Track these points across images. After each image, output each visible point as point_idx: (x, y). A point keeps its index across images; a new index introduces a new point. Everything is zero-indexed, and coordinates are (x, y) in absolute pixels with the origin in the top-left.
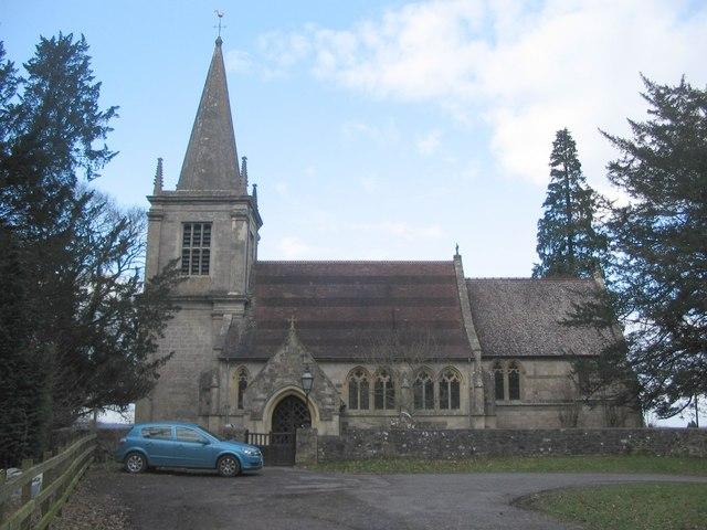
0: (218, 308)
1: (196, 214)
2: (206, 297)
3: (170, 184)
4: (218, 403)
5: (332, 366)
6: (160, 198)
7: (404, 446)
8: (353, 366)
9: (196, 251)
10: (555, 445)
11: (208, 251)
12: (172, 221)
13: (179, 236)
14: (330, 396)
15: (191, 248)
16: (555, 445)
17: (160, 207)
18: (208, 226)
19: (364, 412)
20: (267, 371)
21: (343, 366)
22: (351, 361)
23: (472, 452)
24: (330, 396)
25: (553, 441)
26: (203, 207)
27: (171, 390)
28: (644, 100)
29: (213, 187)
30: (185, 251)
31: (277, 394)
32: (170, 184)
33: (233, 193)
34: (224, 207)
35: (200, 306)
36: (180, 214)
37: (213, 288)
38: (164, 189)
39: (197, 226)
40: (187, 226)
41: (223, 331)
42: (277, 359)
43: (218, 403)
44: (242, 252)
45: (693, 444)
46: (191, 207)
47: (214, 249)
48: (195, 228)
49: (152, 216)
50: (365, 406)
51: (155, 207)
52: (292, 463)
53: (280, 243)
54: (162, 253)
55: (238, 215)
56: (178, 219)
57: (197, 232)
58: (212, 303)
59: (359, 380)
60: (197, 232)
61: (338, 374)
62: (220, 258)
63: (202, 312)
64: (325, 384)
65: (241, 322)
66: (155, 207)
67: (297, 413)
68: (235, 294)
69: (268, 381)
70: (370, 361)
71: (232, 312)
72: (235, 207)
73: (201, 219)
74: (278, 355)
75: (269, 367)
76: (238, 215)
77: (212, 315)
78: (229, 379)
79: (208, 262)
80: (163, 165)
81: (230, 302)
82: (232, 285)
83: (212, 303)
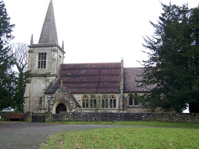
0: (48, 78)
1: (42, 50)
2: (44, 75)
3: (36, 42)
4: (44, 106)
5: (77, 95)
6: (32, 46)
7: (76, 117)
8: (83, 95)
9: (42, 61)
10: (121, 117)
11: (45, 61)
12: (35, 53)
13: (37, 57)
14: (72, 103)
15: (41, 61)
16: (121, 117)
17: (32, 49)
18: (46, 54)
19: (87, 108)
20: (54, 96)
21: (81, 95)
22: (83, 93)
23: (96, 119)
24: (72, 103)
25: (120, 116)
26: (44, 48)
27: (34, 102)
28: (31, 38)
29: (48, 42)
30: (39, 62)
31: (56, 103)
32: (36, 42)
33: (52, 43)
34: (50, 48)
35: (43, 78)
36: (38, 50)
37: (47, 72)
38: (33, 43)
39: (43, 54)
40: (40, 54)
41: (48, 85)
42: (57, 92)
43: (44, 106)
44: (55, 61)
45: (165, 117)
46: (41, 48)
47: (47, 61)
48: (45, 54)
49: (30, 52)
50: (87, 107)
51: (30, 49)
52: (44, 121)
53: (70, 59)
54: (32, 63)
55: (54, 50)
56: (37, 52)
57: (43, 56)
58: (46, 77)
59: (85, 99)
60: (43, 56)
61: (79, 97)
62: (49, 63)
63: (43, 79)
64: (71, 100)
65: (54, 83)
66: (30, 49)
67: (63, 109)
68: (53, 74)
69: (54, 99)
70: (89, 93)
71: (52, 79)
72: (53, 48)
73: (43, 52)
74: (57, 91)
75: (54, 95)
76: (54, 50)
77: (46, 80)
78: (47, 98)
79: (45, 64)
80: (33, 37)
81: (51, 76)
82: (52, 71)
83: (46, 77)
